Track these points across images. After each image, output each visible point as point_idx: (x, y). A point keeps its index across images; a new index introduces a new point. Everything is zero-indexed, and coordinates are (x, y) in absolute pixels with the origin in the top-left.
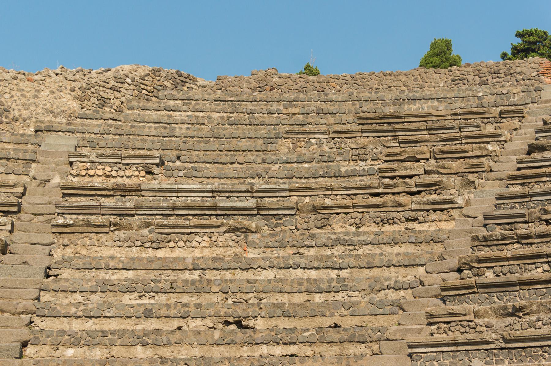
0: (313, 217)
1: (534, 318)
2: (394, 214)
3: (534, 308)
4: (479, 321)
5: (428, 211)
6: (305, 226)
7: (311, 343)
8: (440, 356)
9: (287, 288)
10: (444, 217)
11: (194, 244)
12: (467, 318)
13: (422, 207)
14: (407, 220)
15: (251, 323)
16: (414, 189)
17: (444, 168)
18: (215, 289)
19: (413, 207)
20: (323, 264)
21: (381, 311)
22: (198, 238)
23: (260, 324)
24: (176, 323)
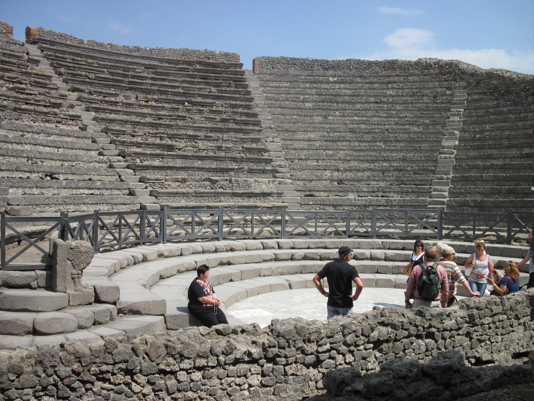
0: (14, 113)
1: (188, 183)
2: (52, 118)
3: (189, 179)
4: (166, 183)
5: (67, 119)
6: (9, 117)
7: (99, 189)
8: (168, 198)
9: (55, 158)
10: (75, 124)
12: (162, 181)
13: (66, 117)
14: (57, 122)
15: (57, 176)
16: (48, 104)
17: (48, 93)
18: (25, 155)
19: (61, 116)
20: (53, 145)
21: (110, 174)
23: (61, 177)
24: (28, 175)
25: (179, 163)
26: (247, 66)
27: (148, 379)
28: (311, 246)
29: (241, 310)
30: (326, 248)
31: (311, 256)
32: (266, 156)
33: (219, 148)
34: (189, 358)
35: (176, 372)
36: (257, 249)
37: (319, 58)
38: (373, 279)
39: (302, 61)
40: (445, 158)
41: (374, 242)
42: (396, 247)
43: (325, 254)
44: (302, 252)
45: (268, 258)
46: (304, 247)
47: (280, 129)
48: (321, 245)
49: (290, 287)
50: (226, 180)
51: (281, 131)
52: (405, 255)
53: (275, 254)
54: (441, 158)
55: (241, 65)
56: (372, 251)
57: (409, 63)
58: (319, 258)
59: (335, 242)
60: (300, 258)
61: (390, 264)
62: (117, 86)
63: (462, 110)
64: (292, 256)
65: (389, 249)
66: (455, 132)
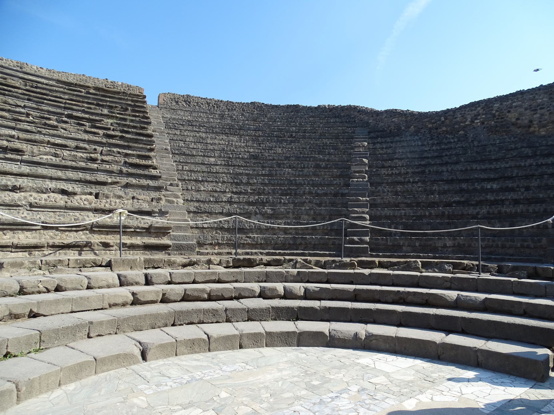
25: (26, 169)
26: (151, 101)
28: (197, 280)
30: (219, 282)
31: (196, 294)
32: (154, 172)
33: (94, 160)
36: (109, 287)
37: (225, 100)
38: (294, 333)
39: (209, 101)
41: (287, 272)
42: (319, 278)
43: (218, 290)
44: (179, 289)
46: (187, 281)
47: (176, 152)
48: (213, 278)
49: (144, 358)
50: (91, 194)
51: (177, 154)
52: (335, 290)
53: (133, 294)
54: (352, 181)
55: (145, 97)
56: (287, 284)
57: (310, 108)
58: (206, 296)
59: (232, 273)
61: (315, 304)
63: (366, 143)
64: (164, 295)
65: (308, 282)
66: (364, 159)
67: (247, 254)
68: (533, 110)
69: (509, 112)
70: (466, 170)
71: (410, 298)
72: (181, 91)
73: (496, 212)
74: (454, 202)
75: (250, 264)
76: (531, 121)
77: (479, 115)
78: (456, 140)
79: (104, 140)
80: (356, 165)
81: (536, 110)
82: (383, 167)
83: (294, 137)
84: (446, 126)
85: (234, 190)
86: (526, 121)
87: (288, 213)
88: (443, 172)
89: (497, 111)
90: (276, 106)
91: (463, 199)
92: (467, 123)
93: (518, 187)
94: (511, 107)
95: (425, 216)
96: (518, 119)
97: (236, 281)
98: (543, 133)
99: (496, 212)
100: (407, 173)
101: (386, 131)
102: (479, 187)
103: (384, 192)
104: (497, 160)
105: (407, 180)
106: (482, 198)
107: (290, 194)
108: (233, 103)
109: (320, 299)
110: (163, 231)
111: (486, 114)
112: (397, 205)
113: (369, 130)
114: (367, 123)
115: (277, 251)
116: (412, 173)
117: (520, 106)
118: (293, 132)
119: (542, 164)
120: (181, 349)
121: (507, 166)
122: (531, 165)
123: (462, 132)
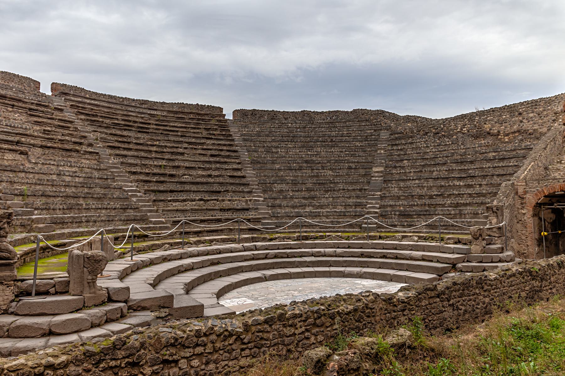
11: (5, 158)
22: (7, 155)
27: (153, 370)
28: (280, 248)
29: (230, 299)
32: (244, 181)
34: (189, 347)
35: (178, 361)
40: (375, 180)
42: (344, 246)
45: (248, 258)
48: (288, 247)
58: (286, 256)
60: (272, 257)
62: (129, 130)
64: (267, 255)
67: (306, 232)
68: (500, 124)
69: (485, 124)
70: (449, 170)
71: (388, 256)
72: (249, 107)
73: (455, 203)
74: (434, 195)
75: (307, 238)
76: (499, 132)
77: (466, 125)
78: (450, 143)
79: (212, 159)
80: (376, 167)
81: (502, 123)
82: (395, 167)
83: (334, 141)
84: (445, 132)
85: (295, 189)
86: (496, 131)
87: (329, 205)
88: (434, 171)
89: (477, 123)
90: (321, 113)
91: (439, 193)
92: (458, 130)
93: (475, 184)
94: (486, 121)
95: (414, 205)
96: (490, 129)
97: (300, 248)
98: (506, 140)
99: (455, 203)
100: (410, 172)
101: (403, 133)
102: (452, 184)
103: (392, 188)
104: (471, 162)
105: (408, 178)
106: (451, 193)
107: (331, 190)
108: (288, 112)
109: (343, 257)
110: (257, 221)
111: (470, 125)
112: (399, 198)
113: (390, 133)
114: (390, 126)
115: (322, 230)
116: (414, 172)
117: (492, 120)
118: (333, 137)
119: (496, 167)
120: (280, 277)
121: (475, 167)
122: (489, 167)
123: (455, 137)
